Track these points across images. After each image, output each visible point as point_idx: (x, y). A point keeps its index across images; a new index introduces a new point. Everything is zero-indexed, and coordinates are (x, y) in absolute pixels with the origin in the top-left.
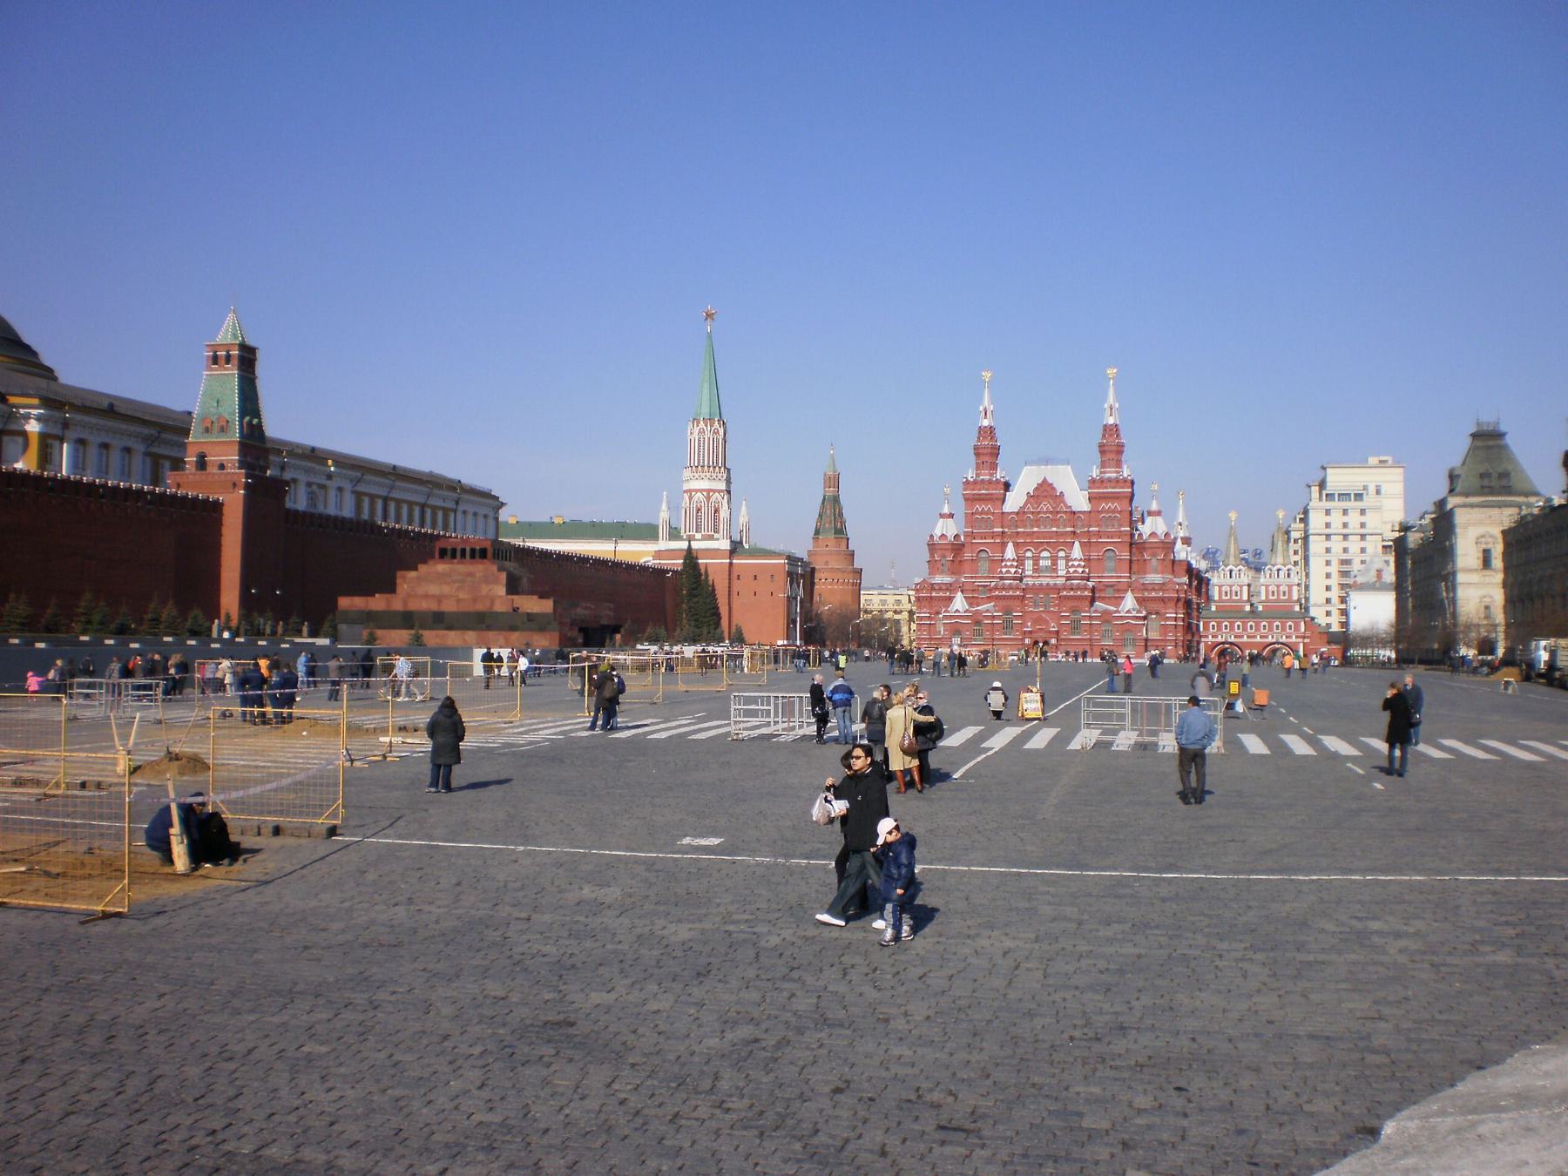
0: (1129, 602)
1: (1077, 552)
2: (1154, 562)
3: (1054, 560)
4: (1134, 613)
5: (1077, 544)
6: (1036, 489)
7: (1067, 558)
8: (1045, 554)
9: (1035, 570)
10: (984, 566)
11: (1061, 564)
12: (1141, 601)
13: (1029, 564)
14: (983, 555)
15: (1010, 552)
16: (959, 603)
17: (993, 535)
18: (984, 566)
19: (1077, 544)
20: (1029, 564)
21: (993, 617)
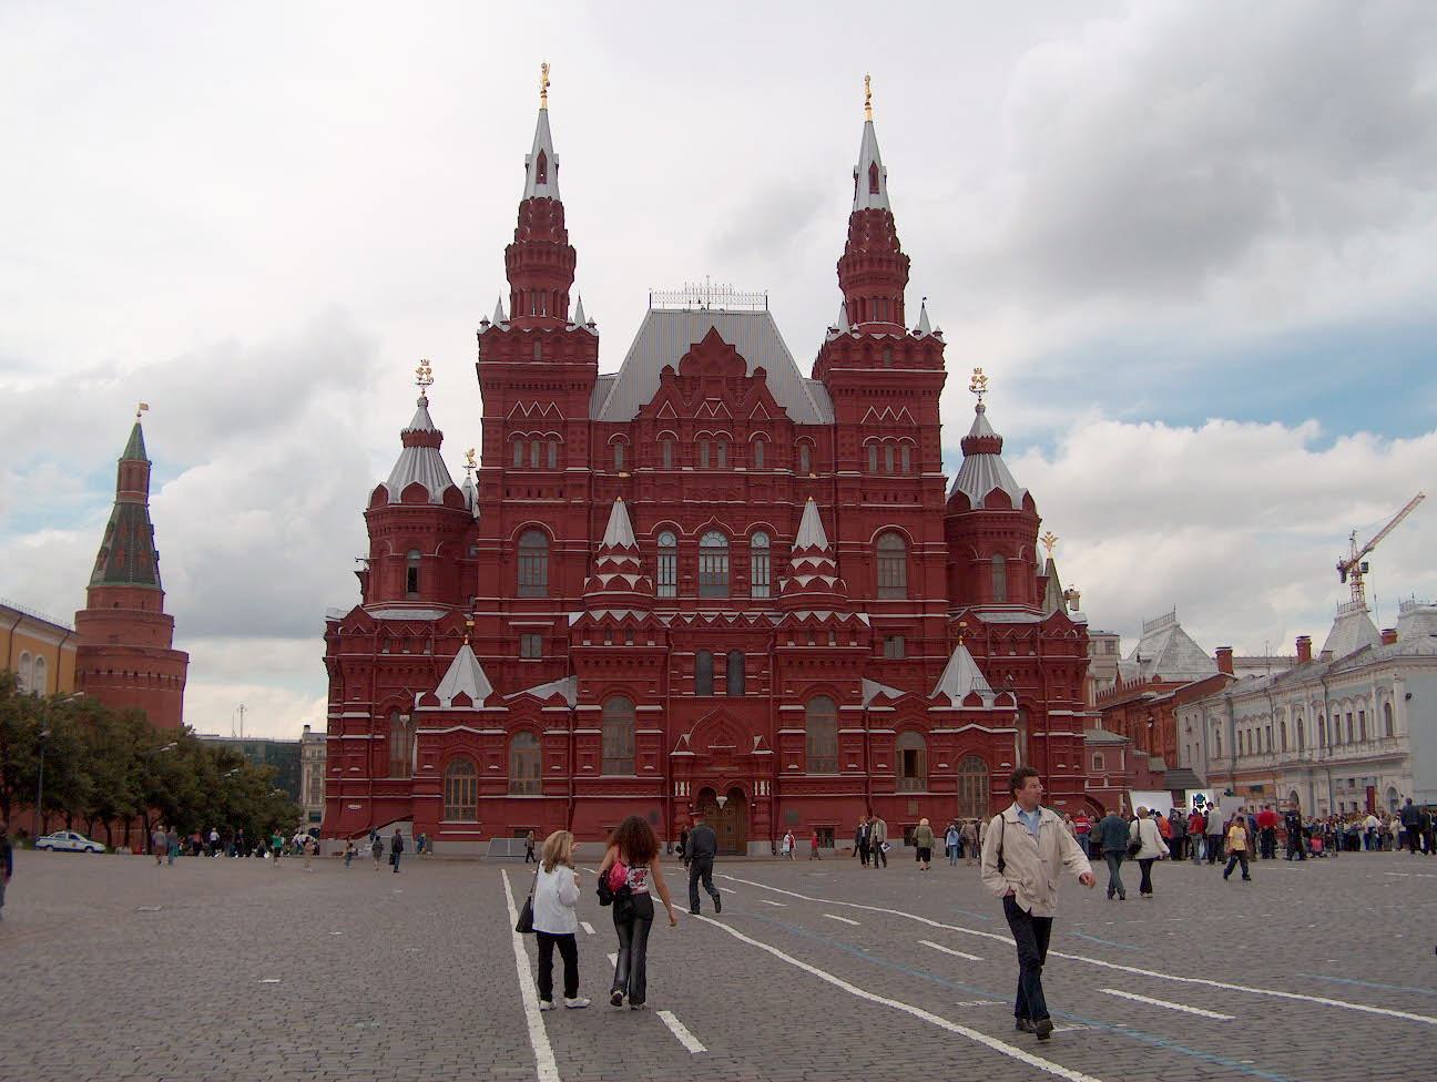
0: (962, 677)
1: (811, 531)
2: (999, 578)
3: (740, 555)
4: (988, 705)
5: (811, 512)
6: (687, 360)
7: (782, 555)
8: (713, 540)
9: (682, 585)
10: (533, 572)
11: (761, 569)
12: (988, 670)
13: (667, 568)
14: (532, 540)
15: (618, 530)
16: (464, 678)
17: (563, 484)
18: (533, 572)
19: (811, 512)
20: (667, 568)
21: (574, 718)
